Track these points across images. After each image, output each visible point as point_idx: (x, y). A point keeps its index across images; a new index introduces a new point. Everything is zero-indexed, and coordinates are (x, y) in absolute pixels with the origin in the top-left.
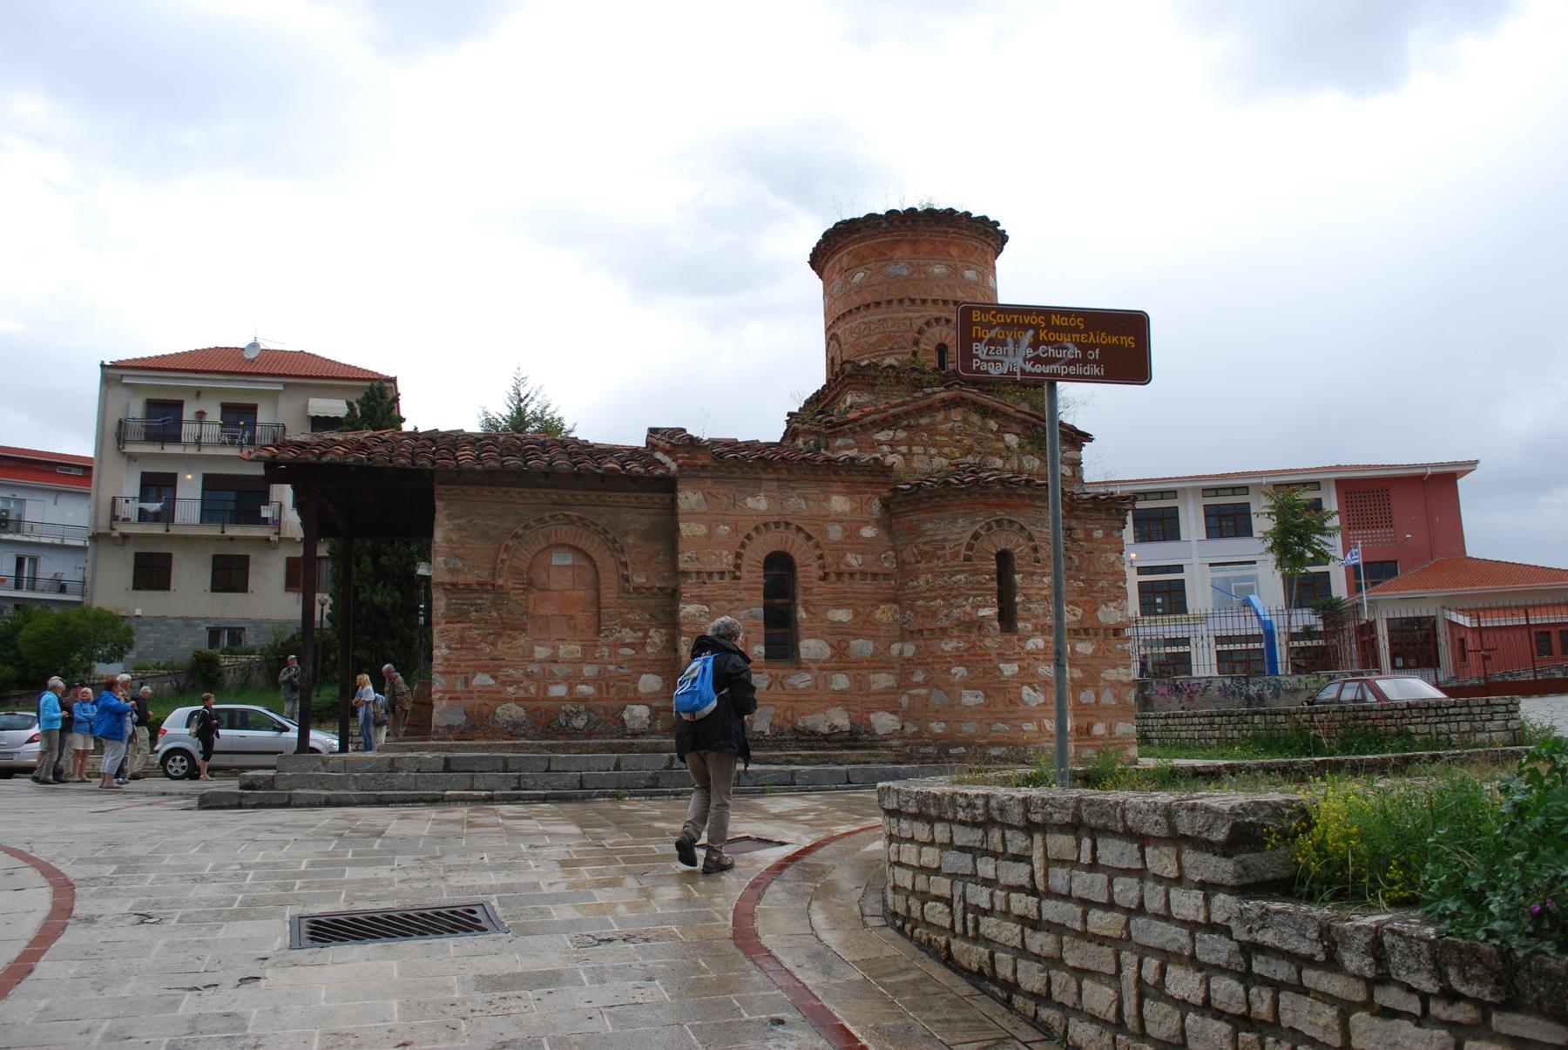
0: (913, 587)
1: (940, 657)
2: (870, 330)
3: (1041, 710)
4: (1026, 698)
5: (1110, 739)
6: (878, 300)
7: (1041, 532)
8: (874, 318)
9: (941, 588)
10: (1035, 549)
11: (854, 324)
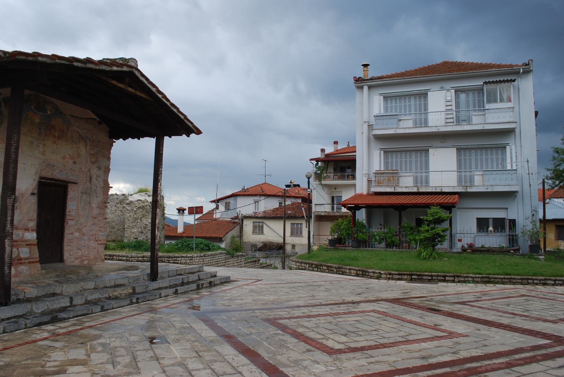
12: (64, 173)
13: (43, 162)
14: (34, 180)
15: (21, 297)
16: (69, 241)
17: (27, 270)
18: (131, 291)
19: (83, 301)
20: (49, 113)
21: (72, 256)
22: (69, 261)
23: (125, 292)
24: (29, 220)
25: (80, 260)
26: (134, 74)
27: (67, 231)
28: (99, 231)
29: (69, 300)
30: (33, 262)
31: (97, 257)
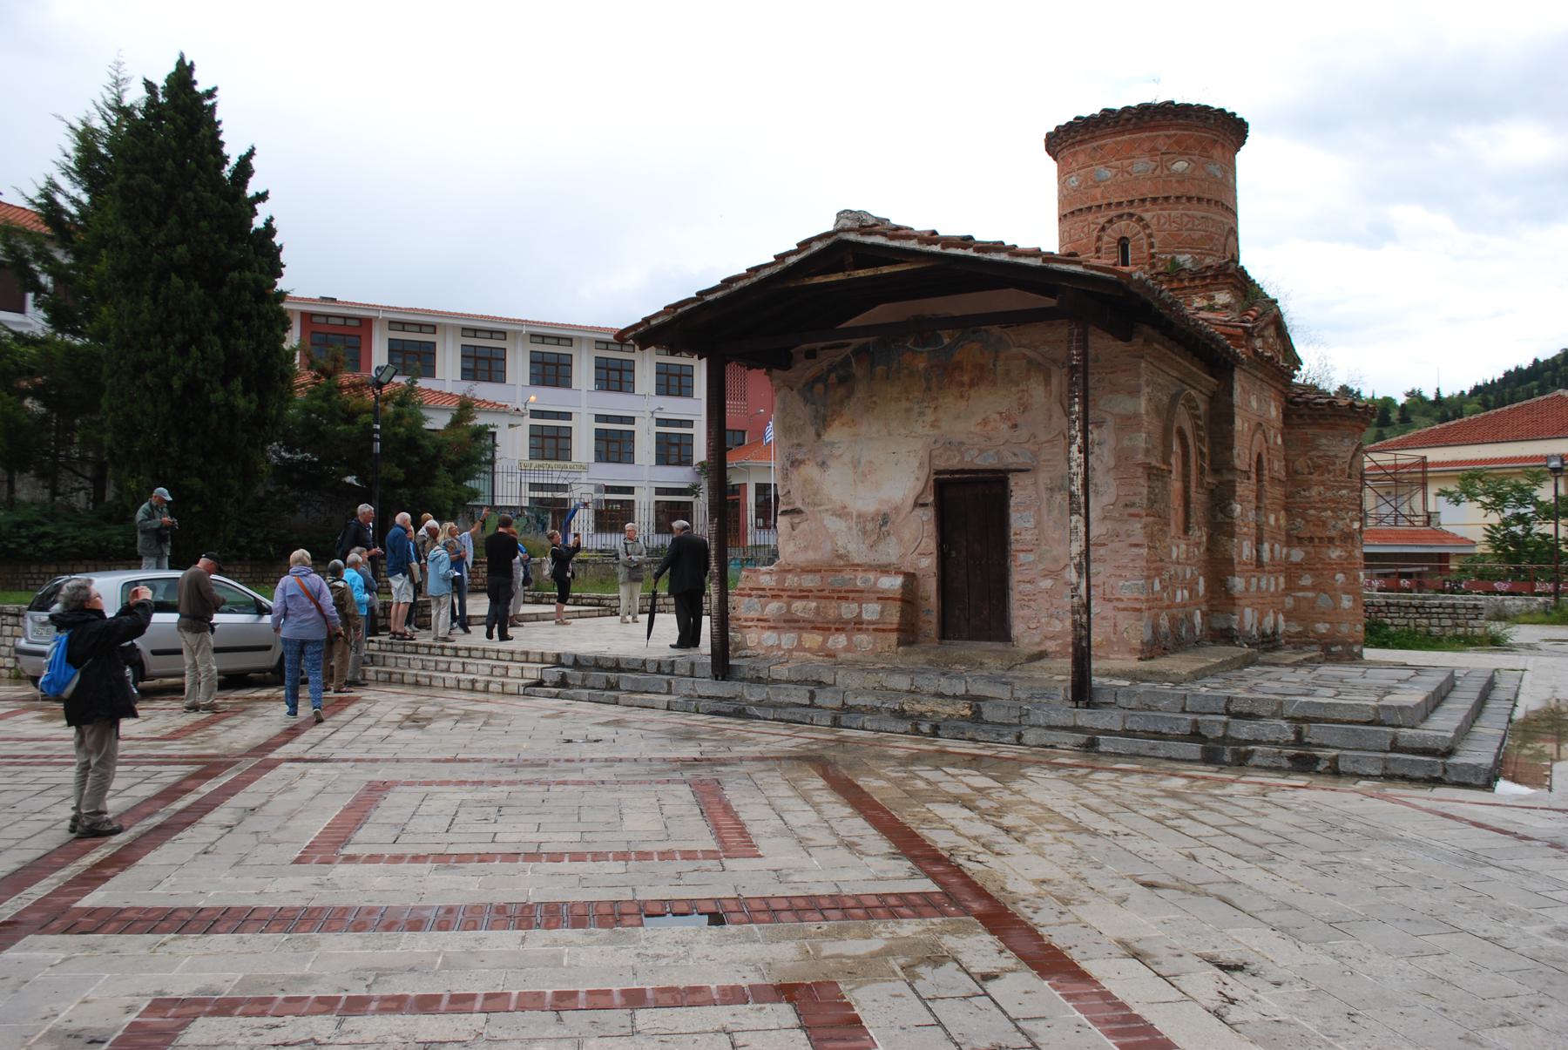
0: (1305, 497)
1: (1330, 564)
2: (1193, 225)
6: (1201, 195)
8: (1198, 214)
9: (1332, 500)
11: (1173, 213)
12: (992, 453)
13: (935, 442)
14: (918, 479)
15: (763, 674)
16: (1026, 598)
17: (869, 643)
18: (967, 712)
19: (838, 704)
20: (946, 341)
21: (1034, 631)
22: (1026, 641)
23: (949, 710)
24: (920, 554)
25: (1060, 642)
26: (848, 242)
27: (1016, 576)
28: (1115, 576)
29: (808, 695)
30: (884, 631)
31: (1115, 640)
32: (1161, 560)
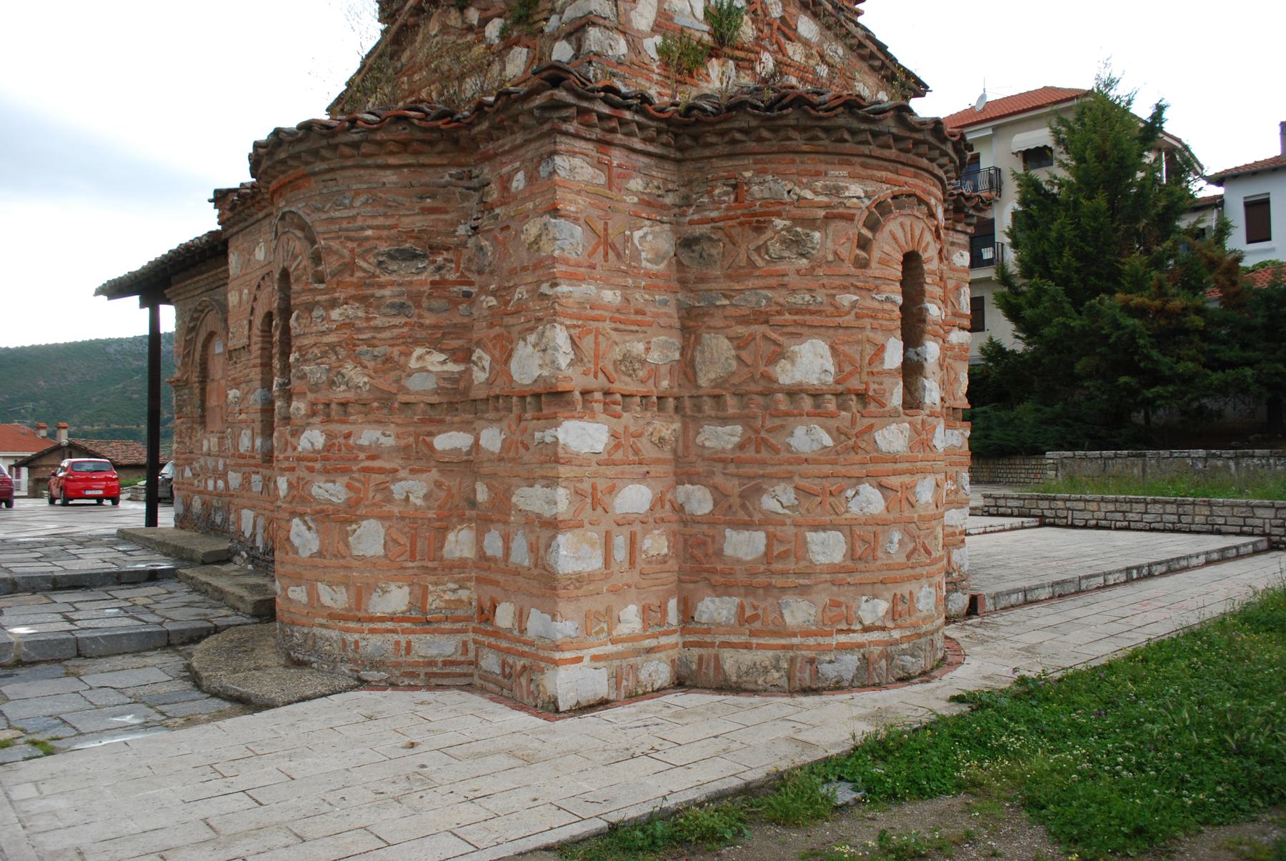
3: (315, 567)
4: (296, 541)
5: (519, 641)
7: (332, 220)
10: (317, 258)
32: (191, 452)
